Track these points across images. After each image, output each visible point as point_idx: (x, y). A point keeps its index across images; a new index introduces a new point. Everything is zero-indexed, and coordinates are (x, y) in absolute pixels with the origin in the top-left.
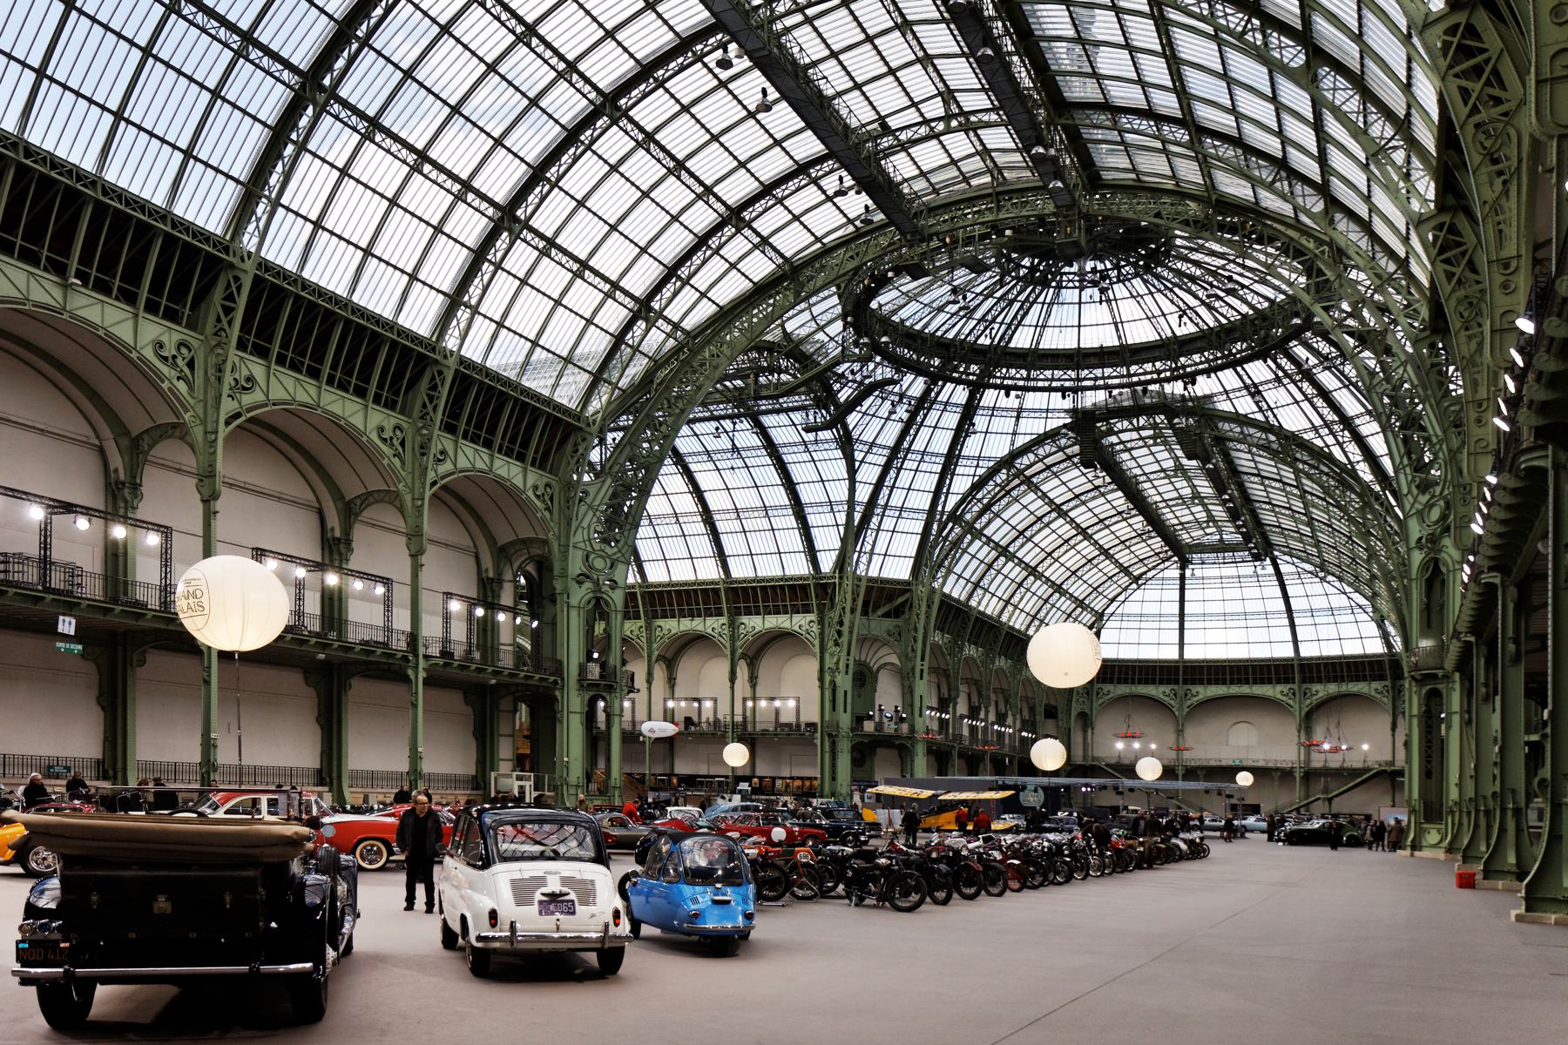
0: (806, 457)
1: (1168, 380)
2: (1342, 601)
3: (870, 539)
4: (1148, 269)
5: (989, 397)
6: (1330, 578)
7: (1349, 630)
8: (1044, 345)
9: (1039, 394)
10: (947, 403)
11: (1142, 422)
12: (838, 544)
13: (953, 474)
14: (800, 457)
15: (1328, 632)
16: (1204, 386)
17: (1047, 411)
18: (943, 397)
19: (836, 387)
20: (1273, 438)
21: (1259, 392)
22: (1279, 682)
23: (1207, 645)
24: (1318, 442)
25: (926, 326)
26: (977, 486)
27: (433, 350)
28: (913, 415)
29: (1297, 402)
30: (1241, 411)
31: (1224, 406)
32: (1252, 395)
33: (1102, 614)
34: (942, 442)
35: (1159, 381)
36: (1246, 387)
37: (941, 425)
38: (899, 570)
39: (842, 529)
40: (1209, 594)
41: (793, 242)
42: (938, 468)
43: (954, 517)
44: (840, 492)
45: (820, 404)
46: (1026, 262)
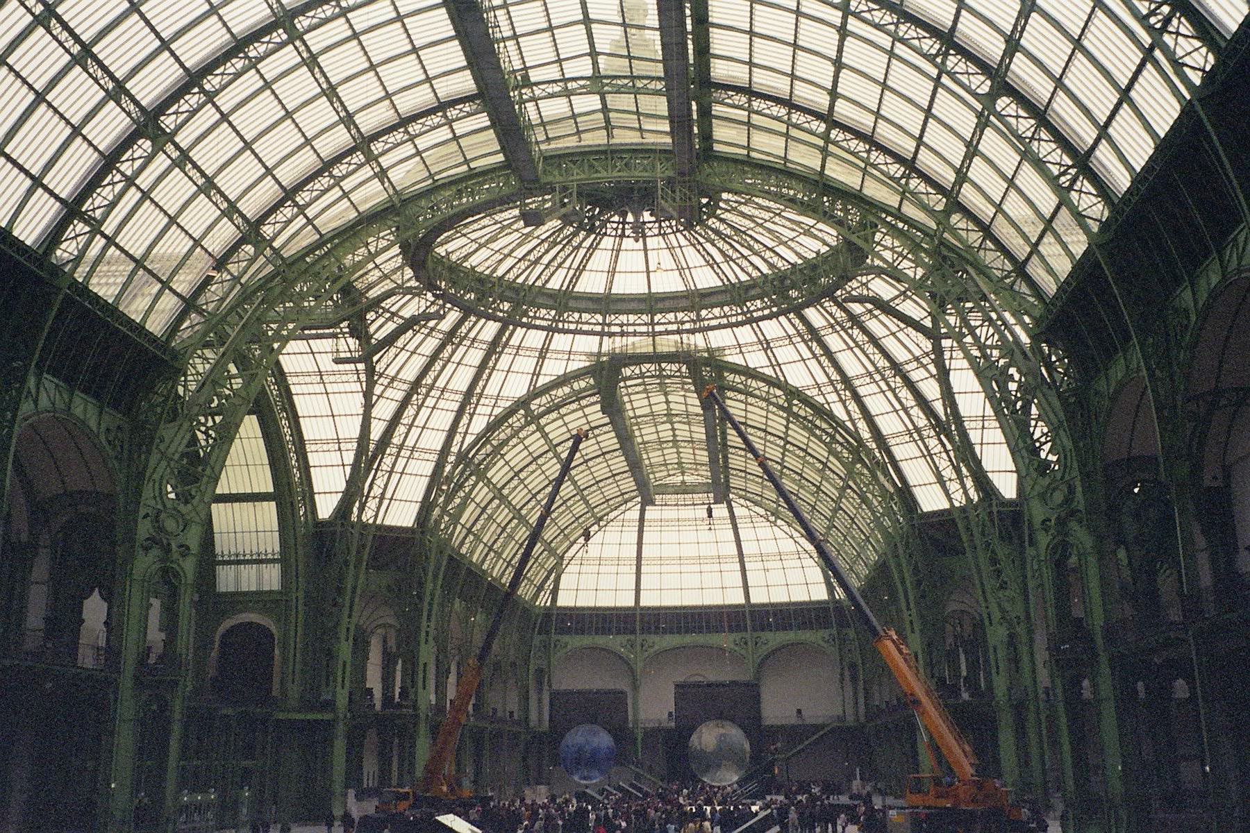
0: (320, 388)
1: (692, 332)
2: (788, 545)
3: (380, 482)
6: (779, 522)
7: (795, 576)
8: (580, 288)
12: (342, 486)
13: (472, 415)
14: (311, 389)
15: (776, 577)
16: (719, 339)
20: (779, 392)
21: (769, 346)
22: (731, 630)
23: (663, 592)
24: (820, 399)
25: (467, 257)
26: (492, 427)
27: (41, 266)
30: (751, 366)
31: (738, 360)
33: (562, 558)
34: (462, 380)
35: (678, 332)
38: (402, 515)
39: (348, 469)
40: (670, 536)
42: (456, 406)
43: (462, 457)
44: (352, 429)
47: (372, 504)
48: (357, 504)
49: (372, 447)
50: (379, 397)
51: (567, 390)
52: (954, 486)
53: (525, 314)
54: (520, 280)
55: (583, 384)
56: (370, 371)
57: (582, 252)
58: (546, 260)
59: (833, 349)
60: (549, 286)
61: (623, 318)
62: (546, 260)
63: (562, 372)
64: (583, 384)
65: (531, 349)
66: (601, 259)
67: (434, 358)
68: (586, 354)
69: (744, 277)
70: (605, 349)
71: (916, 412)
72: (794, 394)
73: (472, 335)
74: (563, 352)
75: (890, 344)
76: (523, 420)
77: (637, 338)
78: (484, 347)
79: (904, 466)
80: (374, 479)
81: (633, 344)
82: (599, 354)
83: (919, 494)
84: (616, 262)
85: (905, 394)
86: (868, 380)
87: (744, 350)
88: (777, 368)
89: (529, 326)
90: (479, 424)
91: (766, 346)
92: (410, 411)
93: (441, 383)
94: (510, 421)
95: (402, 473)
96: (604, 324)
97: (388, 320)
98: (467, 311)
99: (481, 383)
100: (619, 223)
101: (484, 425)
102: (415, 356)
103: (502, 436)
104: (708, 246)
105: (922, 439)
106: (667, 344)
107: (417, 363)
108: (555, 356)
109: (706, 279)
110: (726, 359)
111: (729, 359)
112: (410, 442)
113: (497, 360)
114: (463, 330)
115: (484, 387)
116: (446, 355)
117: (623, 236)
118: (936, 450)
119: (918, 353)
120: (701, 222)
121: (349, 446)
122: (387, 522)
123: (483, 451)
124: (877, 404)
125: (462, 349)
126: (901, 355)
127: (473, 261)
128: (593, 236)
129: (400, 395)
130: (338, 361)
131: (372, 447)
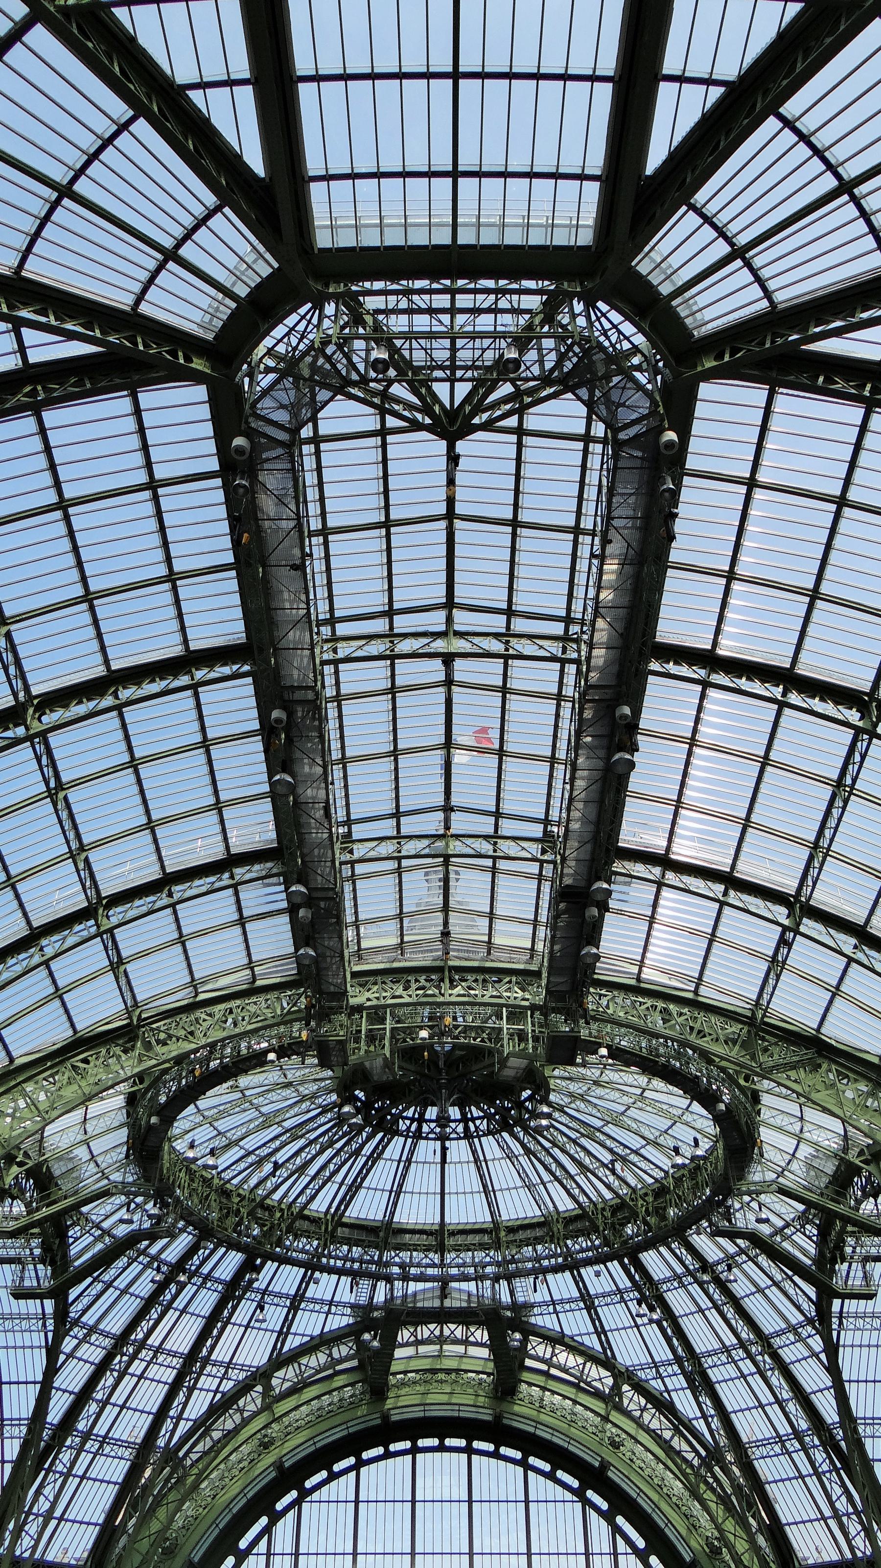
1: (496, 1279)
3: (49, 1491)
4: (505, 1126)
10: (207, 1277)
16: (525, 1290)
17: (331, 1303)
20: (604, 1373)
24: (657, 1384)
26: (216, 1410)
28: (161, 1287)
30: (567, 1332)
35: (479, 1278)
41: (158, 980)
43: (171, 1456)
47: (32, 1528)
48: (11, 1526)
49: (46, 1434)
50: (70, 1356)
51: (322, 1358)
52: (854, 1528)
53: (279, 1243)
54: (277, 1196)
55: (344, 1350)
56: (61, 1314)
57: (361, 1160)
58: (312, 1170)
59: (678, 1310)
60: (314, 1206)
61: (405, 1256)
62: (312, 1170)
63: (317, 1332)
64: (344, 1350)
65: (279, 1295)
66: (382, 1175)
67: (150, 1302)
68: (353, 1306)
70: (380, 1297)
71: (792, 1407)
72: (624, 1376)
73: (205, 1270)
74: (322, 1302)
75: (755, 1306)
76: (259, 1402)
77: (420, 1286)
78: (220, 1287)
79: (772, 1490)
80: (42, 1486)
81: (415, 1294)
82: (370, 1306)
83: (792, 1533)
84: (404, 1176)
85: (776, 1379)
87: (558, 1308)
89: (283, 1260)
90: (199, 1404)
91: (588, 1301)
92: (109, 1380)
93: (154, 1340)
94: (241, 1403)
95: (83, 1477)
96: (379, 1263)
97: (98, 1239)
98: (205, 1233)
99: (209, 1343)
100: (412, 1120)
101: (204, 1408)
103: (229, 1425)
105: (804, 1449)
106: (464, 1292)
107: (128, 1307)
108: (311, 1306)
109: (517, 1207)
110: (533, 1320)
111: (537, 1320)
112: (101, 1429)
113: (234, 1308)
114: (196, 1260)
115: (213, 1347)
116: (168, 1297)
117: (418, 1136)
118: (825, 1467)
119: (795, 1317)
121: (16, 1431)
122: (50, 1557)
123: (199, 1448)
124: (733, 1396)
125: (189, 1290)
126: (769, 1323)
127: (224, 1161)
128: (380, 1135)
129: (96, 1354)
130: (17, 1296)
131: (46, 1434)
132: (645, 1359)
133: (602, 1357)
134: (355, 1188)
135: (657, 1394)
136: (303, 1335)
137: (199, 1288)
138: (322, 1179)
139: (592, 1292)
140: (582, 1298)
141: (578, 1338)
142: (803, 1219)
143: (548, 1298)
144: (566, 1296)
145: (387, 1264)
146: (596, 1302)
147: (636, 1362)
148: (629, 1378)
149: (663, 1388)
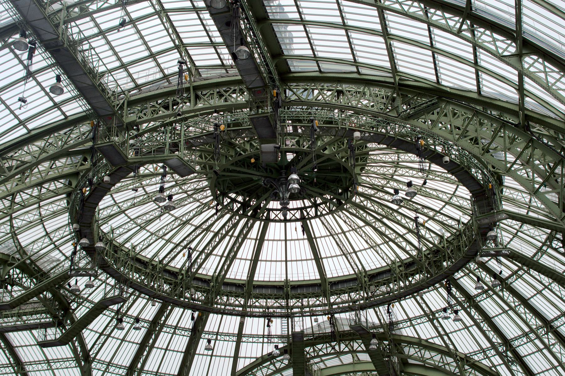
4: (340, 206)
5: (213, 322)
9: (256, 319)
11: (343, 346)
18: (172, 320)
19: (74, 306)
20: (450, 360)
24: (486, 362)
25: (156, 255)
29: (467, 328)
30: (423, 337)
32: (431, 321)
36: (426, 315)
37: (172, 347)
45: (60, 324)
46: (240, 199)
63: (259, 355)
69: (404, 256)
74: (258, 336)
75: (538, 302)
86: (525, 340)
88: (446, 338)
102: (125, 344)
104: (368, 229)
109: (372, 262)
120: (349, 200)
130: (43, 344)
132: (476, 348)
133: (447, 350)
134: (255, 261)
135: (488, 369)
136: (251, 358)
137: (173, 334)
138: (231, 257)
139: (433, 309)
140: (426, 315)
141: (431, 341)
142: (551, 238)
143: (406, 318)
144: (417, 314)
145: (292, 307)
146: (437, 315)
147: (471, 351)
148: (467, 361)
149: (491, 365)
